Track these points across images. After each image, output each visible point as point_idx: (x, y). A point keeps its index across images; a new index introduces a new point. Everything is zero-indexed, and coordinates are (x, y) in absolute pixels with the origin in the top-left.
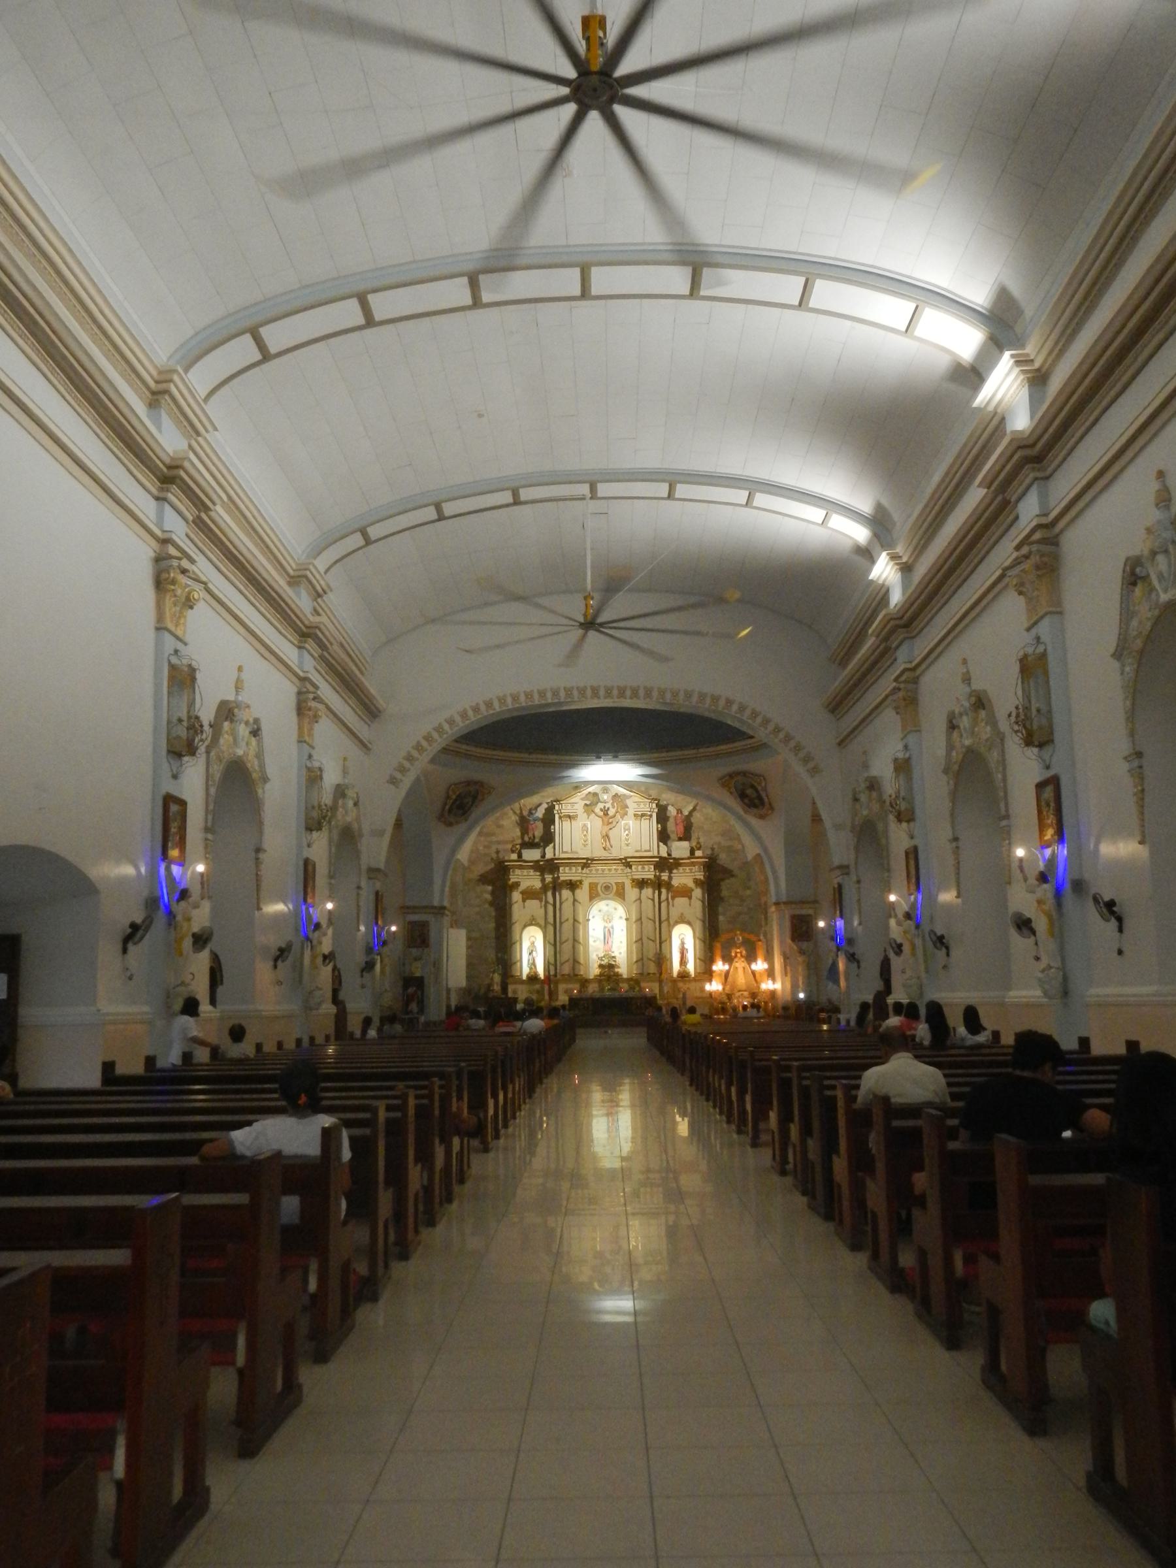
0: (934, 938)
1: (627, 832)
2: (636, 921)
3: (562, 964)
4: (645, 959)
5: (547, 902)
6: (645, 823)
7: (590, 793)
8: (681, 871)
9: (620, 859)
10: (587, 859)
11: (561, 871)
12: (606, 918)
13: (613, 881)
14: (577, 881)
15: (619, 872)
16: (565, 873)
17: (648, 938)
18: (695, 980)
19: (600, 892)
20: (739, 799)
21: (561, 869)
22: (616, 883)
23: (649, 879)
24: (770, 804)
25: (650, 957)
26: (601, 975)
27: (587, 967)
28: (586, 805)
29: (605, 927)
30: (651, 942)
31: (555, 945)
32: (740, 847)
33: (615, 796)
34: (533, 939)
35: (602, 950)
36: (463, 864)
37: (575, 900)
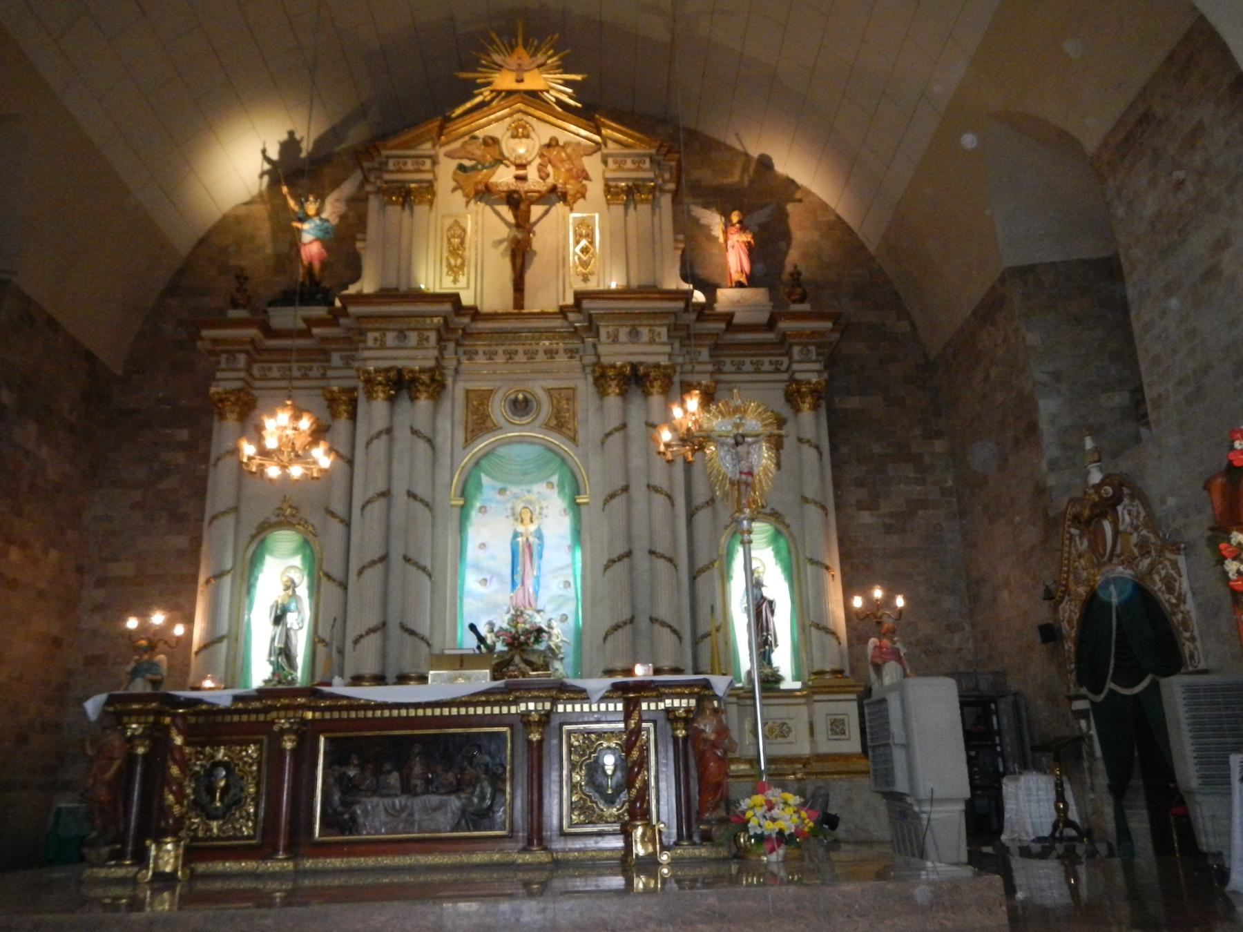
1: (584, 243)
3: (356, 642)
4: (643, 622)
7: (475, 138)
8: (748, 367)
9: (563, 311)
10: (454, 298)
11: (370, 343)
12: (519, 508)
13: (537, 389)
14: (422, 371)
15: (562, 359)
16: (383, 347)
17: (652, 552)
19: (502, 422)
21: (371, 336)
22: (549, 391)
25: (663, 612)
28: (461, 168)
29: (516, 535)
30: (661, 564)
31: (344, 586)
32: (904, 326)
33: (549, 146)
34: (296, 576)
35: (505, 608)
36: (90, 357)
37: (414, 432)
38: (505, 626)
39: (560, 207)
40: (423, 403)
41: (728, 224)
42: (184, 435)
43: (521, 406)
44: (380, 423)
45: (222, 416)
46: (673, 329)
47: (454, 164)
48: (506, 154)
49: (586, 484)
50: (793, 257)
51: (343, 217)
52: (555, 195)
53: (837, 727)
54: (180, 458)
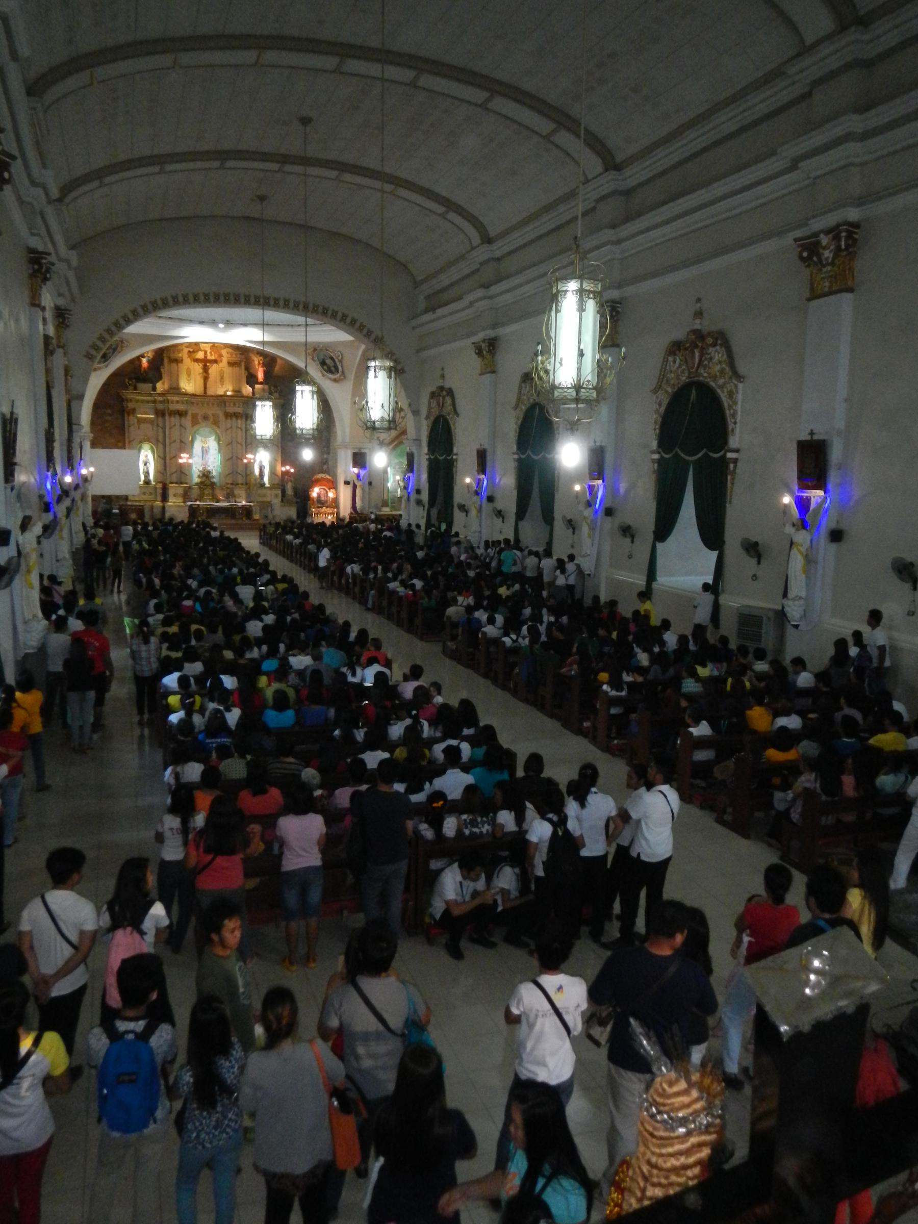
0: (496, 512)
2: (228, 445)
3: (172, 474)
5: (158, 426)
6: (236, 369)
13: (210, 412)
18: (270, 488)
19: (200, 420)
20: (319, 366)
22: (213, 415)
23: (239, 413)
24: (343, 372)
26: (202, 483)
27: (191, 476)
28: (189, 351)
29: (203, 447)
37: (181, 426)
38: (201, 469)
39: (215, 365)
40: (183, 419)
41: (259, 363)
42: (109, 411)
43: (206, 418)
44: (173, 424)
45: (129, 415)
46: (243, 403)
47: (187, 350)
48: (202, 349)
49: (222, 439)
50: (277, 368)
51: (154, 357)
52: (215, 361)
53: (276, 496)
54: (109, 418)
